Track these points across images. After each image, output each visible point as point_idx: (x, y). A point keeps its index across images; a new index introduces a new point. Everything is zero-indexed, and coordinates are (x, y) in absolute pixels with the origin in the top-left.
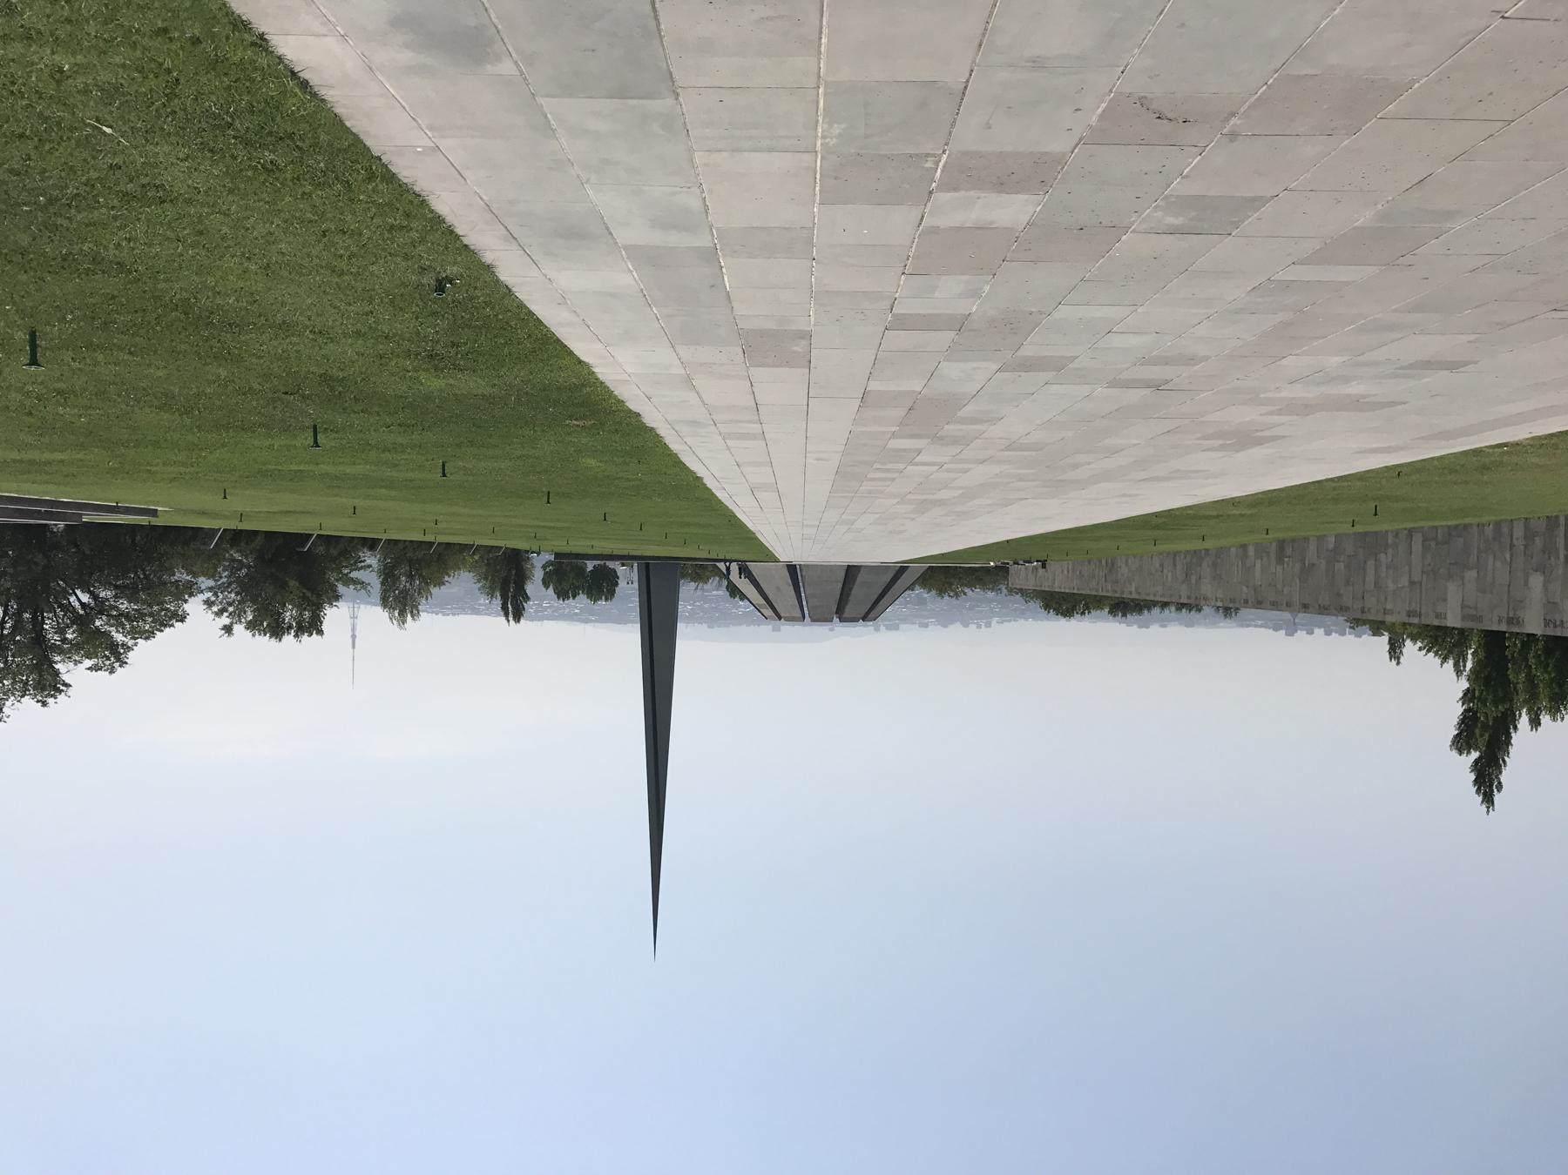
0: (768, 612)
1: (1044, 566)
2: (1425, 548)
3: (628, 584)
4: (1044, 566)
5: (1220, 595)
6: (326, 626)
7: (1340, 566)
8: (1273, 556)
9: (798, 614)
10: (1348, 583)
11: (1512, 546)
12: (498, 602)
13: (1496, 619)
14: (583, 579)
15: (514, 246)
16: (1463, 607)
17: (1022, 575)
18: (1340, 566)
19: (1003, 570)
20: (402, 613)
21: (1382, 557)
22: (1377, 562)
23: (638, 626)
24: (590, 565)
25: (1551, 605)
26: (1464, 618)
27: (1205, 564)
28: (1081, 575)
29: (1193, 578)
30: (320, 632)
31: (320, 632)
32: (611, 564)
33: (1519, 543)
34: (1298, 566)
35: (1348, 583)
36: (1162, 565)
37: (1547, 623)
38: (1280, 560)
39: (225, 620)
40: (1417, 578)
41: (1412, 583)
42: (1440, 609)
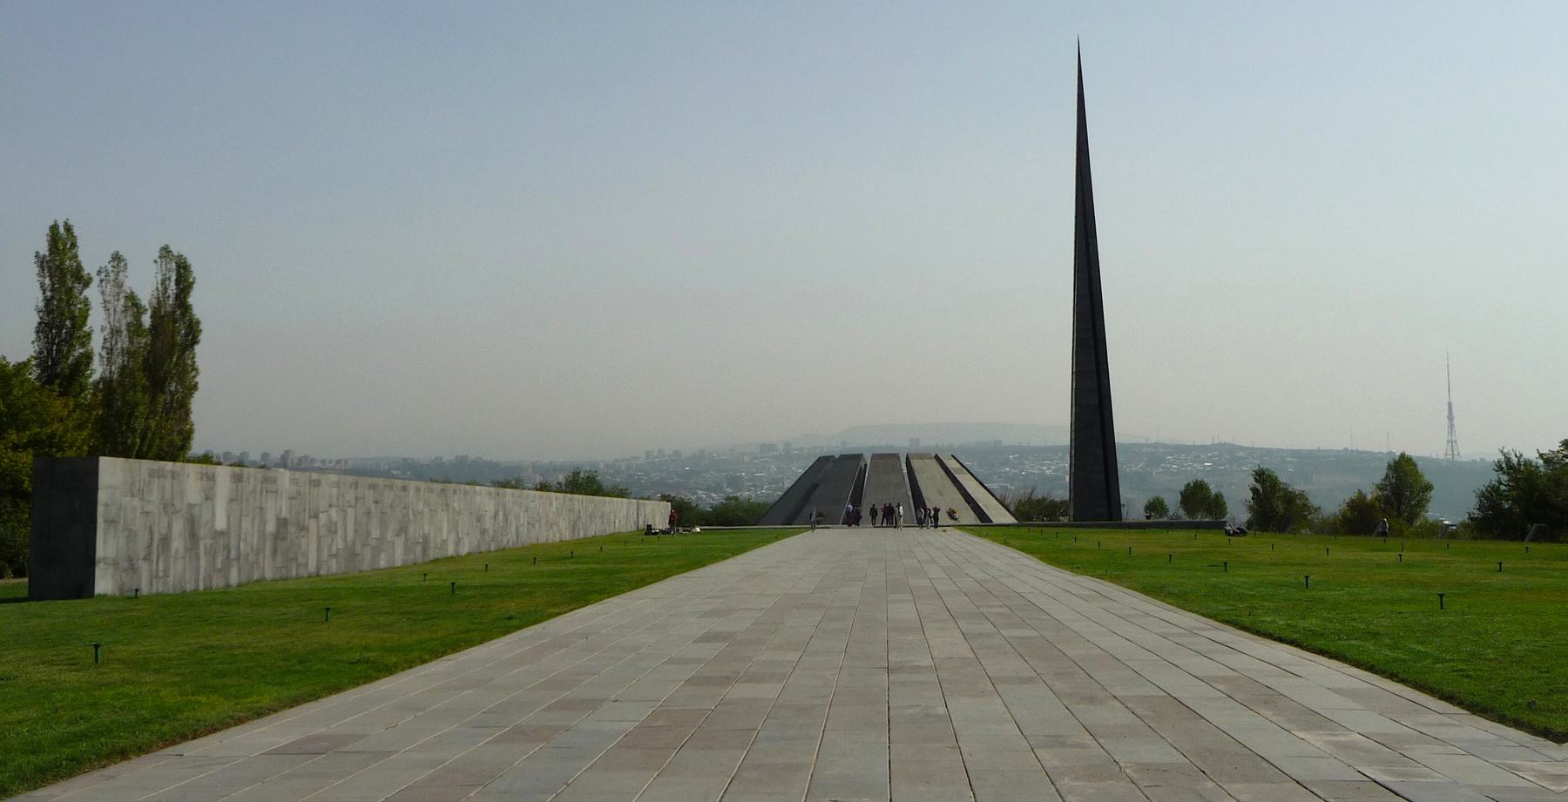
0: (952, 465)
2: (306, 556)
9: (915, 464)
15: (1296, 771)
17: (658, 513)
18: (375, 533)
21: (341, 545)
22: (345, 540)
25: (209, 496)
26: (274, 481)
27: (491, 533)
34: (411, 529)
35: (369, 513)
37: (211, 478)
38: (426, 539)
41: (316, 516)
42: (294, 489)
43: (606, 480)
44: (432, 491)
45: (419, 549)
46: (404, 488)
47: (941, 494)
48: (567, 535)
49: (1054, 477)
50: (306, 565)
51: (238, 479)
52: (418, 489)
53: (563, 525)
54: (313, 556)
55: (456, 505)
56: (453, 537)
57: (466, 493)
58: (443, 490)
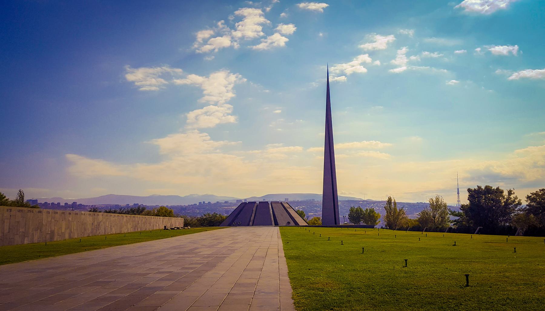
0: (286, 205)
3: (344, 215)
4: (165, 227)
5: (83, 216)
6: (467, 194)
10: (18, 222)
14: (362, 217)
17: (178, 222)
19: (186, 224)
20: (437, 201)
24: (362, 223)
28: (150, 224)
29: (96, 223)
30: (469, 190)
31: (469, 190)
36: (111, 229)
38: (52, 232)
39: (512, 196)
44: (57, 213)
45: (48, 236)
47: (282, 215)
53: (129, 226)
55: (70, 219)
56: (68, 231)
57: (76, 214)
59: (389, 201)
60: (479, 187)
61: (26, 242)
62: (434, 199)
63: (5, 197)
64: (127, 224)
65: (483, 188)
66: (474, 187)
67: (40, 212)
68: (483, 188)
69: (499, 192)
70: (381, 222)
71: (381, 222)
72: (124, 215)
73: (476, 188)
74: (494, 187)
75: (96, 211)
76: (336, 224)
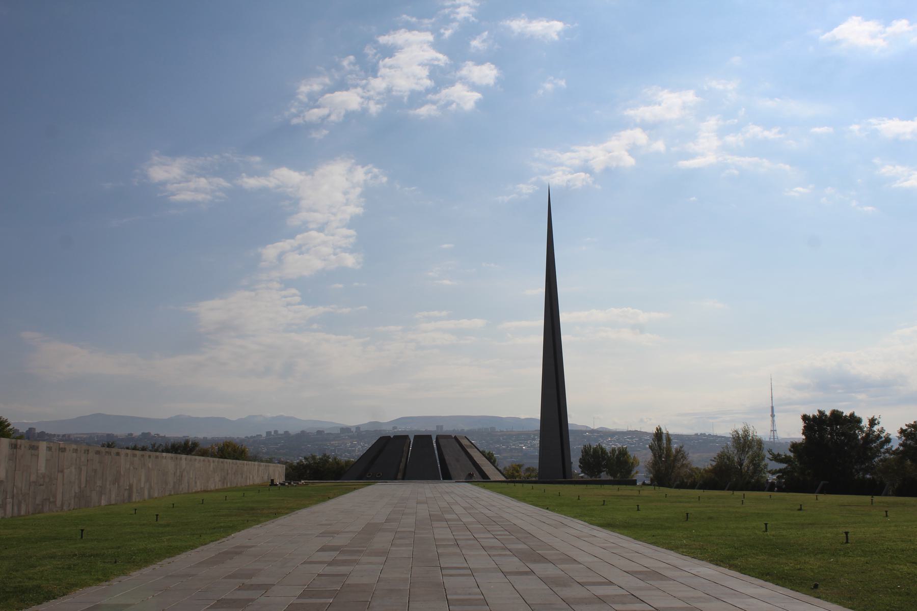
0: (465, 442)
1: (272, 481)
5: (164, 461)
6: (801, 425)
7: (99, 483)
8: (135, 490)
9: (441, 441)
10: (95, 471)
11: (13, 498)
12: (675, 446)
13: (23, 447)
16: (38, 456)
17: (278, 473)
18: (99, 483)
23: (570, 428)
24: (604, 476)
30: (805, 418)
31: (805, 418)
32: (587, 478)
33: (9, 500)
35: (95, 471)
38: (131, 486)
39: (876, 428)
40: (60, 475)
41: (62, 471)
43: (250, 450)
44: (134, 455)
45: (126, 494)
46: (118, 454)
48: (219, 486)
49: (529, 452)
50: (55, 502)
51: (14, 446)
52: (127, 455)
54: (59, 497)
55: (150, 465)
57: (157, 457)
58: (143, 456)
59: (659, 435)
60: (821, 413)
61: (103, 503)
62: (741, 432)
63: (9, 425)
64: (203, 475)
65: (828, 413)
66: (812, 412)
67: (118, 454)
68: (828, 413)
69: (854, 420)
70: (641, 474)
71: (641, 474)
72: (211, 459)
73: (816, 413)
74: (847, 413)
75: (156, 451)
76: (565, 477)
